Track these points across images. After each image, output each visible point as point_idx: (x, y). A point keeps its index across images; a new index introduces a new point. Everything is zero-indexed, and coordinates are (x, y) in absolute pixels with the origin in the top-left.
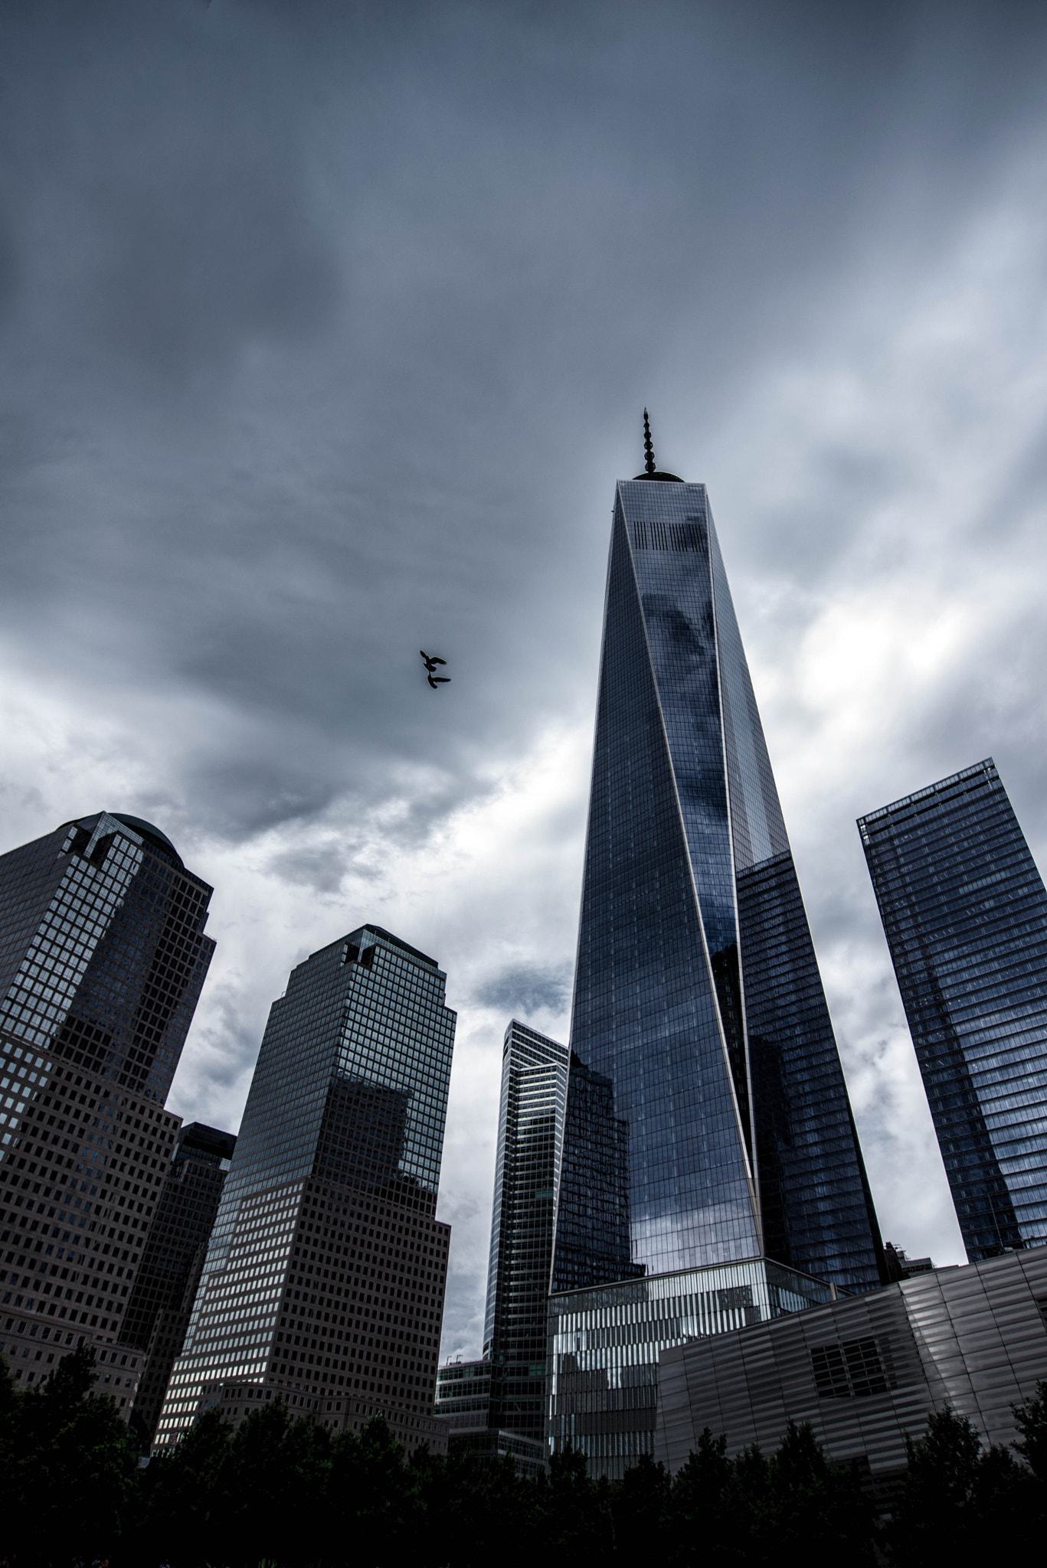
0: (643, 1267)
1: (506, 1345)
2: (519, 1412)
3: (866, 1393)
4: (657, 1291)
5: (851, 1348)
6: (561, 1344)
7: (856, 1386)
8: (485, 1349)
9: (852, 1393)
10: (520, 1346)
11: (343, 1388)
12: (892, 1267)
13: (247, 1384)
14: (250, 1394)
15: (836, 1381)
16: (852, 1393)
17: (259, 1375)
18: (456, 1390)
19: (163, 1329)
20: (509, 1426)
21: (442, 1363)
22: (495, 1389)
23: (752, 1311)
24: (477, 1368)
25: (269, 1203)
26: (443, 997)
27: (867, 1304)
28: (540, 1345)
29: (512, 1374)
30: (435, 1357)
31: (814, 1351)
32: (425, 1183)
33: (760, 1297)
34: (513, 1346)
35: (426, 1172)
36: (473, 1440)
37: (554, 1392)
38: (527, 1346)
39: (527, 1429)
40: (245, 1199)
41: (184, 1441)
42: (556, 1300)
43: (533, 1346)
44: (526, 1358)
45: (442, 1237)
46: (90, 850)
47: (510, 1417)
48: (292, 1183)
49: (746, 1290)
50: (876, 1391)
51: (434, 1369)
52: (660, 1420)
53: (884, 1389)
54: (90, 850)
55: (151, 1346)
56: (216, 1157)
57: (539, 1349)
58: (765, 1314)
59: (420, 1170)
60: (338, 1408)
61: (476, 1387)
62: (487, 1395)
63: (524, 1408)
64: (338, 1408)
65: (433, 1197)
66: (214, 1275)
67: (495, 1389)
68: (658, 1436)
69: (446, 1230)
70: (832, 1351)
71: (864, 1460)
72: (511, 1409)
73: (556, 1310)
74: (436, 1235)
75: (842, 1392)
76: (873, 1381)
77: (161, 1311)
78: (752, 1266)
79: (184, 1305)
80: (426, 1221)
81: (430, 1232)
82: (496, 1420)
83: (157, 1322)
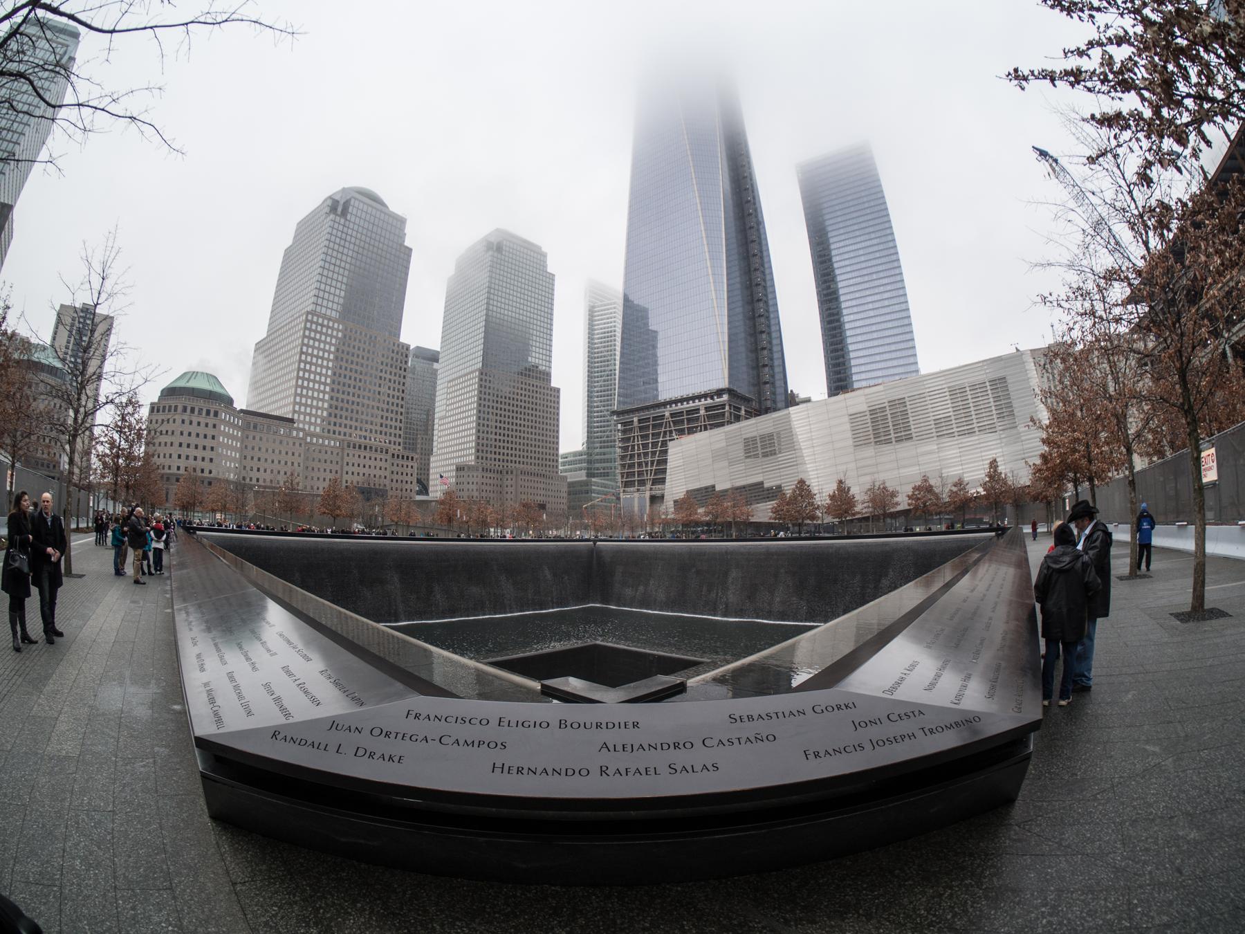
5: (763, 438)
12: (791, 400)
18: (570, 463)
21: (562, 451)
22: (589, 462)
24: (580, 454)
26: (545, 266)
36: (580, 483)
41: (1082, 351)
46: (340, 209)
54: (340, 209)
61: (581, 461)
65: (549, 375)
66: (440, 419)
67: (589, 462)
69: (558, 390)
71: (762, 483)
75: (756, 456)
82: (590, 475)
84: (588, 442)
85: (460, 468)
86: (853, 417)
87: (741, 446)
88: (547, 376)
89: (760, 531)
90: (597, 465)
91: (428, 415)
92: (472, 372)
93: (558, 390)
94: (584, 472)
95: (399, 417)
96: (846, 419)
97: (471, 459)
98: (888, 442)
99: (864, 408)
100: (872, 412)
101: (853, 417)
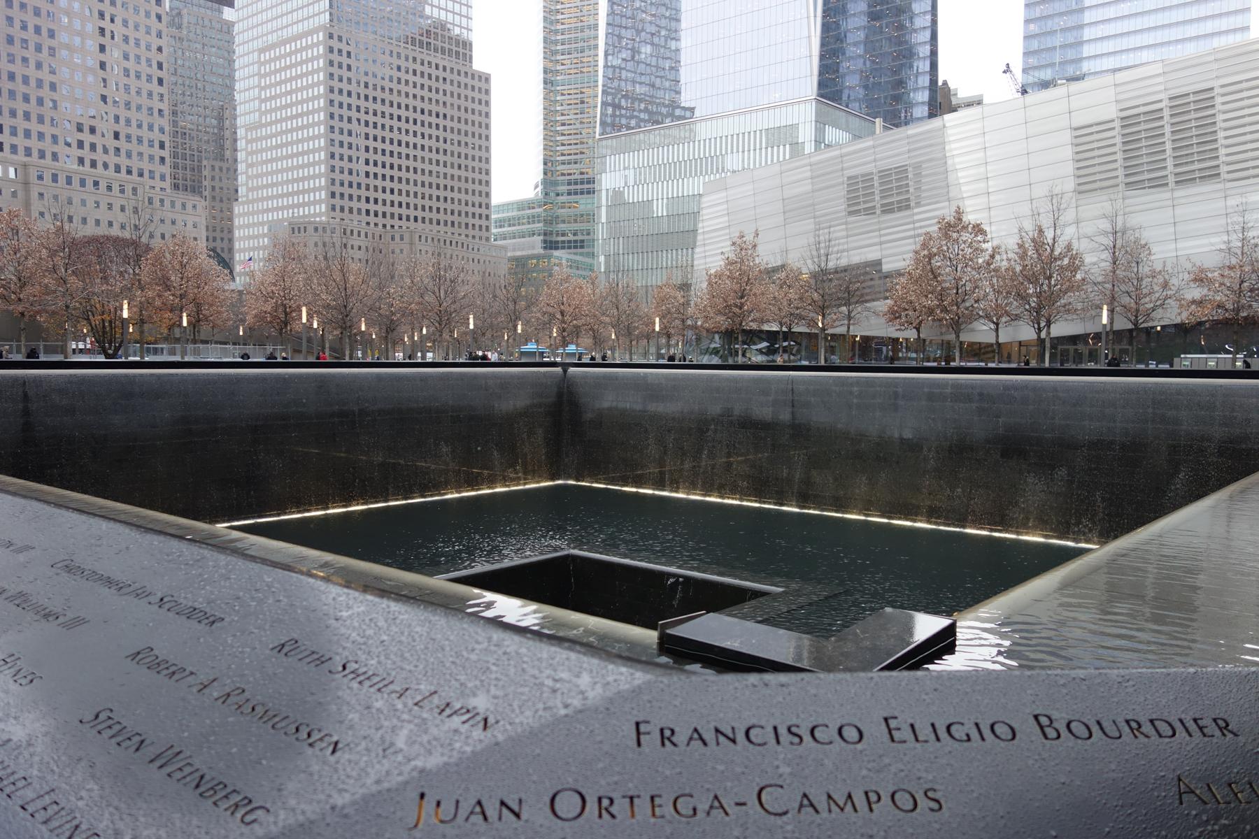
0: (692, 110)
1: (555, 183)
2: (571, 237)
3: (891, 211)
4: (704, 131)
5: (885, 175)
6: (608, 182)
7: (883, 206)
8: (536, 187)
9: (878, 212)
10: (569, 184)
11: (404, 223)
12: (941, 102)
13: (310, 223)
14: (316, 229)
15: (865, 202)
16: (878, 212)
17: (320, 215)
18: (511, 222)
19: (213, 179)
20: (563, 248)
23: (796, 147)
24: (529, 204)
25: (290, 54)
27: (908, 137)
28: (589, 182)
29: (563, 207)
30: (488, 195)
31: (849, 178)
32: (457, 31)
33: (806, 134)
34: (563, 184)
35: (457, 17)
37: (604, 220)
38: (576, 183)
39: (579, 250)
40: (262, 51)
42: (604, 143)
43: (582, 183)
44: (576, 193)
45: (483, 85)
47: (563, 242)
48: (310, 33)
49: (794, 127)
50: (900, 209)
51: (488, 206)
52: (700, 238)
53: (908, 207)
55: (206, 193)
56: (216, 6)
57: (586, 186)
58: (809, 148)
59: (450, 16)
60: (402, 239)
61: (532, 219)
62: (541, 225)
63: (575, 235)
64: (402, 239)
65: (467, 45)
66: (250, 128)
68: (697, 250)
70: (867, 178)
71: (878, 263)
72: (563, 235)
73: (604, 151)
74: (476, 83)
75: (870, 211)
76: (899, 202)
77: (205, 162)
78: (802, 106)
79: (228, 153)
80: (463, 70)
81: (469, 81)
82: (550, 245)
83: (205, 173)
84: (545, 182)
85: (297, 228)
86: (1081, 133)
87: (842, 191)
88: (462, 49)
89: (868, 353)
90: (562, 227)
91: (221, 119)
92: (310, 33)
93: (487, 80)
94: (538, 240)
95: (158, 122)
96: (1067, 136)
97: (317, 210)
98: (1159, 183)
99: (1111, 112)
100: (1127, 121)
101: (1081, 133)
